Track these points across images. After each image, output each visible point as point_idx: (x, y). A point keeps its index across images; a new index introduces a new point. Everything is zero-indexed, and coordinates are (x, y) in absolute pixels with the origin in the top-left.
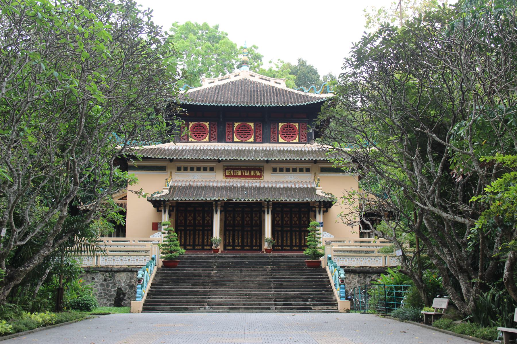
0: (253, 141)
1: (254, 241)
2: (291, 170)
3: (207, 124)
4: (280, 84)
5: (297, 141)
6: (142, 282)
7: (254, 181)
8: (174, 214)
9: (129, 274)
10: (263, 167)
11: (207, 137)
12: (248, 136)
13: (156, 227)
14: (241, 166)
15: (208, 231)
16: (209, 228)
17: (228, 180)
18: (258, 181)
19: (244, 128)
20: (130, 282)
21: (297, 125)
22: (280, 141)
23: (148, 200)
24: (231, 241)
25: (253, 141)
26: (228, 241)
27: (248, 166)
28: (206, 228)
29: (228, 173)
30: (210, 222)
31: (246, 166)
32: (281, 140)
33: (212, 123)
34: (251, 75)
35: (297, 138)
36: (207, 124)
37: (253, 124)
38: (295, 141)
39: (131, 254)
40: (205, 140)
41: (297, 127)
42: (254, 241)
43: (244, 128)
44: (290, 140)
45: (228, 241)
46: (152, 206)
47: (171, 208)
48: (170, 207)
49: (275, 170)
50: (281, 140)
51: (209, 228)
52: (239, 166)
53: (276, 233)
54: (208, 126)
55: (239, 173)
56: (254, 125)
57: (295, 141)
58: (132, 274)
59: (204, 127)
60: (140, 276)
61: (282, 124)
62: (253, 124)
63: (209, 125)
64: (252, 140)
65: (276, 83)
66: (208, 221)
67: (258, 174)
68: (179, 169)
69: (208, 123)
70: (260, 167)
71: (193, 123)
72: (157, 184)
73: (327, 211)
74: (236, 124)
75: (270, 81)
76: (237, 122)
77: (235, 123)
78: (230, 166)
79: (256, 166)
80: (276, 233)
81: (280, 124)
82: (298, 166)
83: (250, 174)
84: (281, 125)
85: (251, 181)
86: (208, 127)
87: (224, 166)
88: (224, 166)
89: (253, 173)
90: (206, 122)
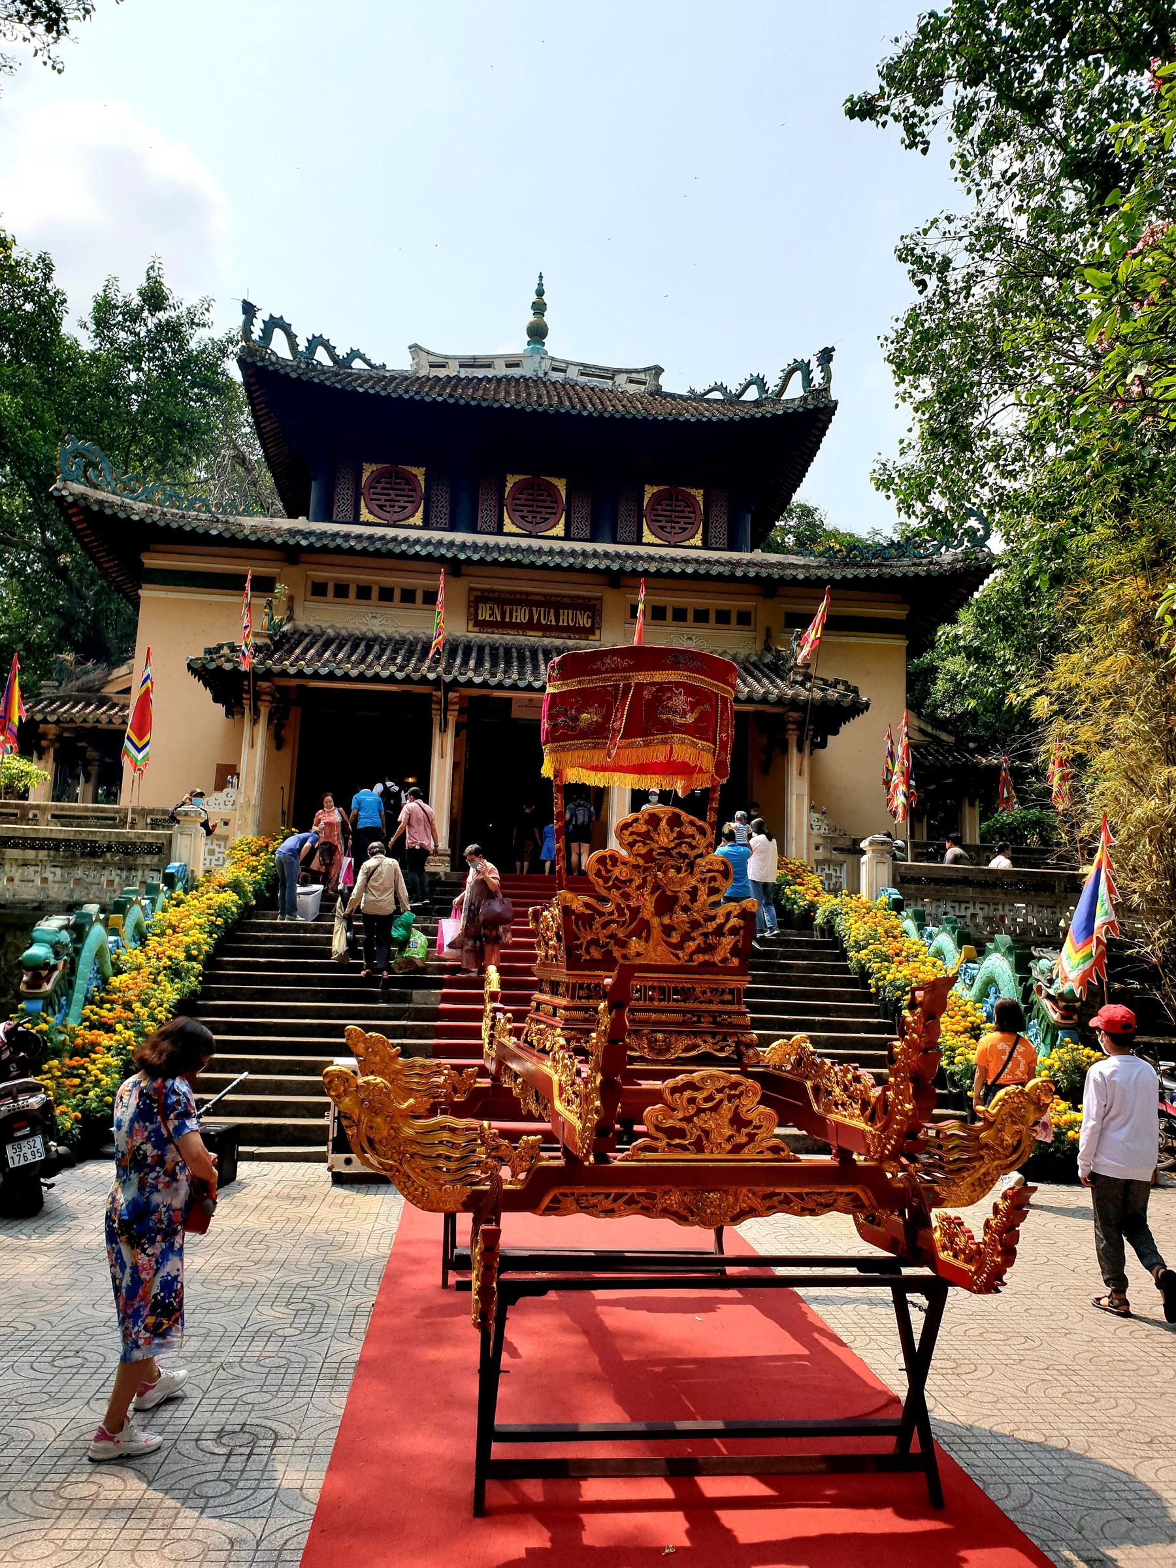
0: (562, 534)
2: (690, 616)
3: (419, 473)
5: (699, 543)
6: (48, 987)
11: (419, 514)
12: (548, 520)
13: (225, 775)
14: (528, 594)
22: (644, 540)
23: (189, 667)
25: (562, 534)
31: (545, 595)
35: (699, 536)
36: (419, 473)
37: (564, 481)
38: (692, 542)
40: (411, 521)
41: (700, 499)
46: (208, 694)
52: (521, 593)
54: (421, 479)
55: (521, 616)
57: (692, 542)
59: (410, 480)
61: (655, 489)
62: (564, 481)
65: (631, 381)
67: (584, 621)
68: (319, 590)
70: (589, 599)
72: (234, 626)
73: (823, 745)
74: (511, 481)
76: (514, 472)
77: (509, 477)
81: (647, 487)
82: (714, 604)
83: (557, 620)
86: (423, 483)
88: (471, 589)
90: (418, 466)
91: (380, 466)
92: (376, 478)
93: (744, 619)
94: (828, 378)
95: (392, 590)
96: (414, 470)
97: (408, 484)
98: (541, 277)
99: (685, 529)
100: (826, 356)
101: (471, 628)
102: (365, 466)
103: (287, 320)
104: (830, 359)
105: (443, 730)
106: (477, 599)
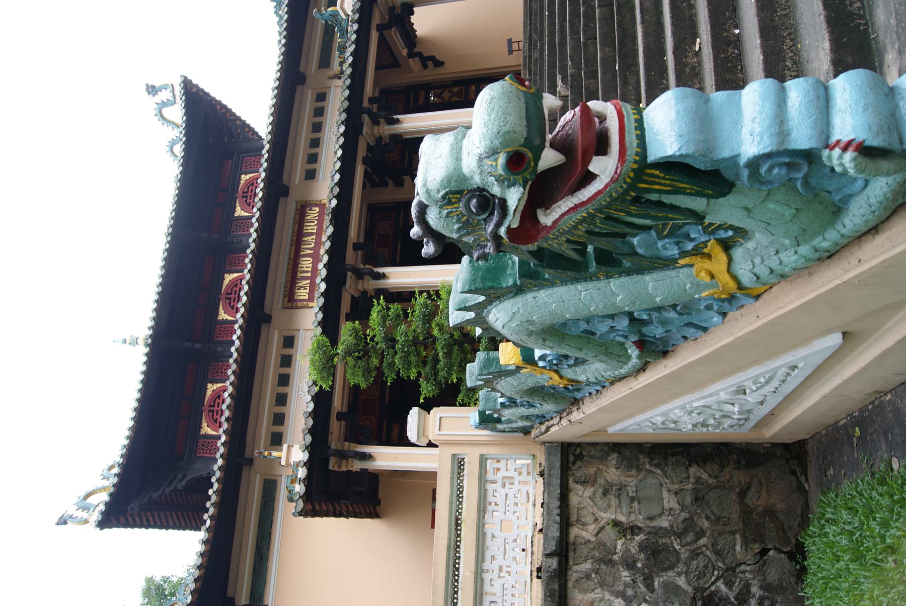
9: (581, 567)
14: (290, 259)
19: (233, 296)
20: (630, 565)
31: (291, 245)
37: (226, 275)
41: (248, 176)
52: (289, 264)
56: (230, 272)
58: (583, 551)
61: (238, 208)
69: (209, 385)
71: (204, 424)
76: (218, 315)
81: (236, 214)
83: (312, 234)
87: (284, 308)
90: (206, 389)
91: (204, 420)
93: (322, 97)
94: (165, 87)
95: (280, 375)
96: (209, 392)
98: (114, 341)
100: (152, 90)
102: (203, 432)
103: (83, 494)
104: (153, 87)
105: (384, 276)
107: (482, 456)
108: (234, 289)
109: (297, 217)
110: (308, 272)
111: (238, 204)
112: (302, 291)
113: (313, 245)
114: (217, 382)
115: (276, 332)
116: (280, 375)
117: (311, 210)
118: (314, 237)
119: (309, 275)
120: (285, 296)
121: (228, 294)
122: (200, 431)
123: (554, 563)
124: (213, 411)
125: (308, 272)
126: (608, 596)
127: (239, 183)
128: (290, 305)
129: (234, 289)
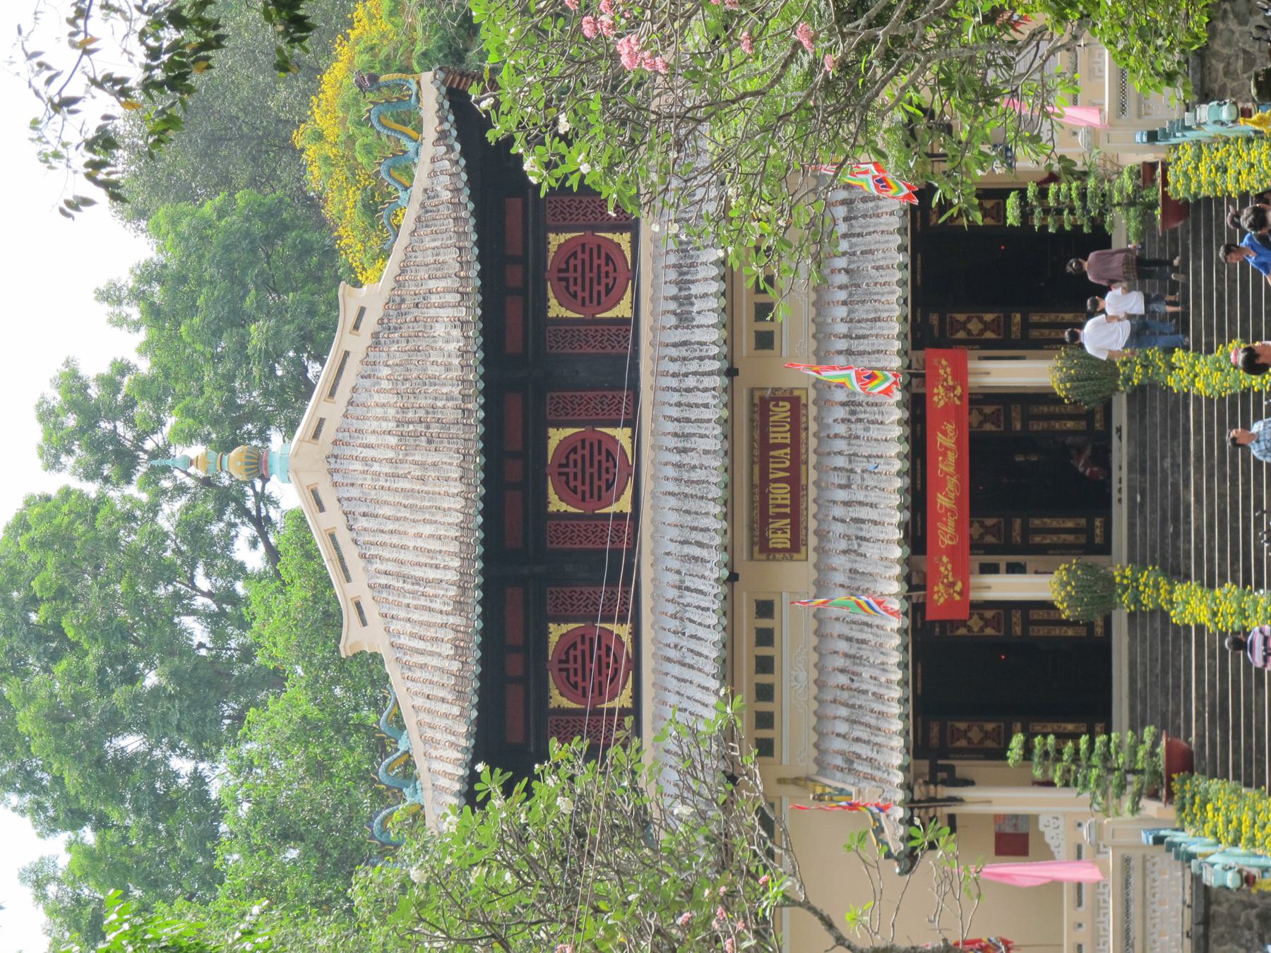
1: (1070, 425)
4: (362, 310)
7: (813, 427)
8: (963, 768)
9: (1215, 932)
10: (752, 391)
14: (752, 485)
15: (1027, 623)
16: (1017, 616)
17: (813, 541)
18: (813, 411)
21: (555, 240)
22: (628, 314)
24: (1070, 524)
25: (628, 431)
26: (1070, 538)
27: (751, 455)
28: (1018, 630)
29: (780, 540)
30: (989, 614)
31: (752, 463)
32: (623, 310)
33: (550, 610)
34: (316, 435)
35: (616, 237)
38: (626, 248)
39: (1136, 932)
41: (563, 237)
42: (1070, 425)
43: (571, 470)
44: (619, 265)
45: (1070, 538)
47: (942, 775)
48: (933, 781)
49: (765, 341)
50: (623, 310)
51: (1017, 616)
52: (752, 494)
53: (1035, 334)
55: (780, 493)
57: (626, 248)
59: (569, 643)
60: (1231, 880)
61: (553, 302)
63: (559, 620)
64: (622, 435)
65: (356, 327)
66: (987, 623)
67: (781, 412)
69: (552, 627)
70: (752, 404)
71: (554, 692)
75: (347, 354)
76: (546, 503)
78: (751, 529)
79: (752, 420)
80: (1035, 334)
81: (551, 314)
83: (783, 446)
84: (555, 310)
85: (813, 443)
88: (751, 557)
89: (780, 435)
90: (545, 634)
91: (552, 685)
92: (573, 688)
95: (757, 657)
97: (574, 646)
99: (608, 258)
101: (803, 556)
106: (762, 547)
107: (1144, 857)
108: (572, 457)
109: (757, 416)
110: (785, 506)
111: (551, 294)
112: (779, 534)
113: (788, 464)
114: (567, 621)
115: (744, 594)
116: (757, 657)
117: (777, 405)
118: (788, 451)
119: (788, 510)
120: (752, 544)
121: (560, 466)
122: (547, 703)
123: (1201, 929)
124: (567, 670)
125: (785, 506)
126: (1235, 948)
127: (547, 250)
128: (764, 556)
129: (572, 457)
